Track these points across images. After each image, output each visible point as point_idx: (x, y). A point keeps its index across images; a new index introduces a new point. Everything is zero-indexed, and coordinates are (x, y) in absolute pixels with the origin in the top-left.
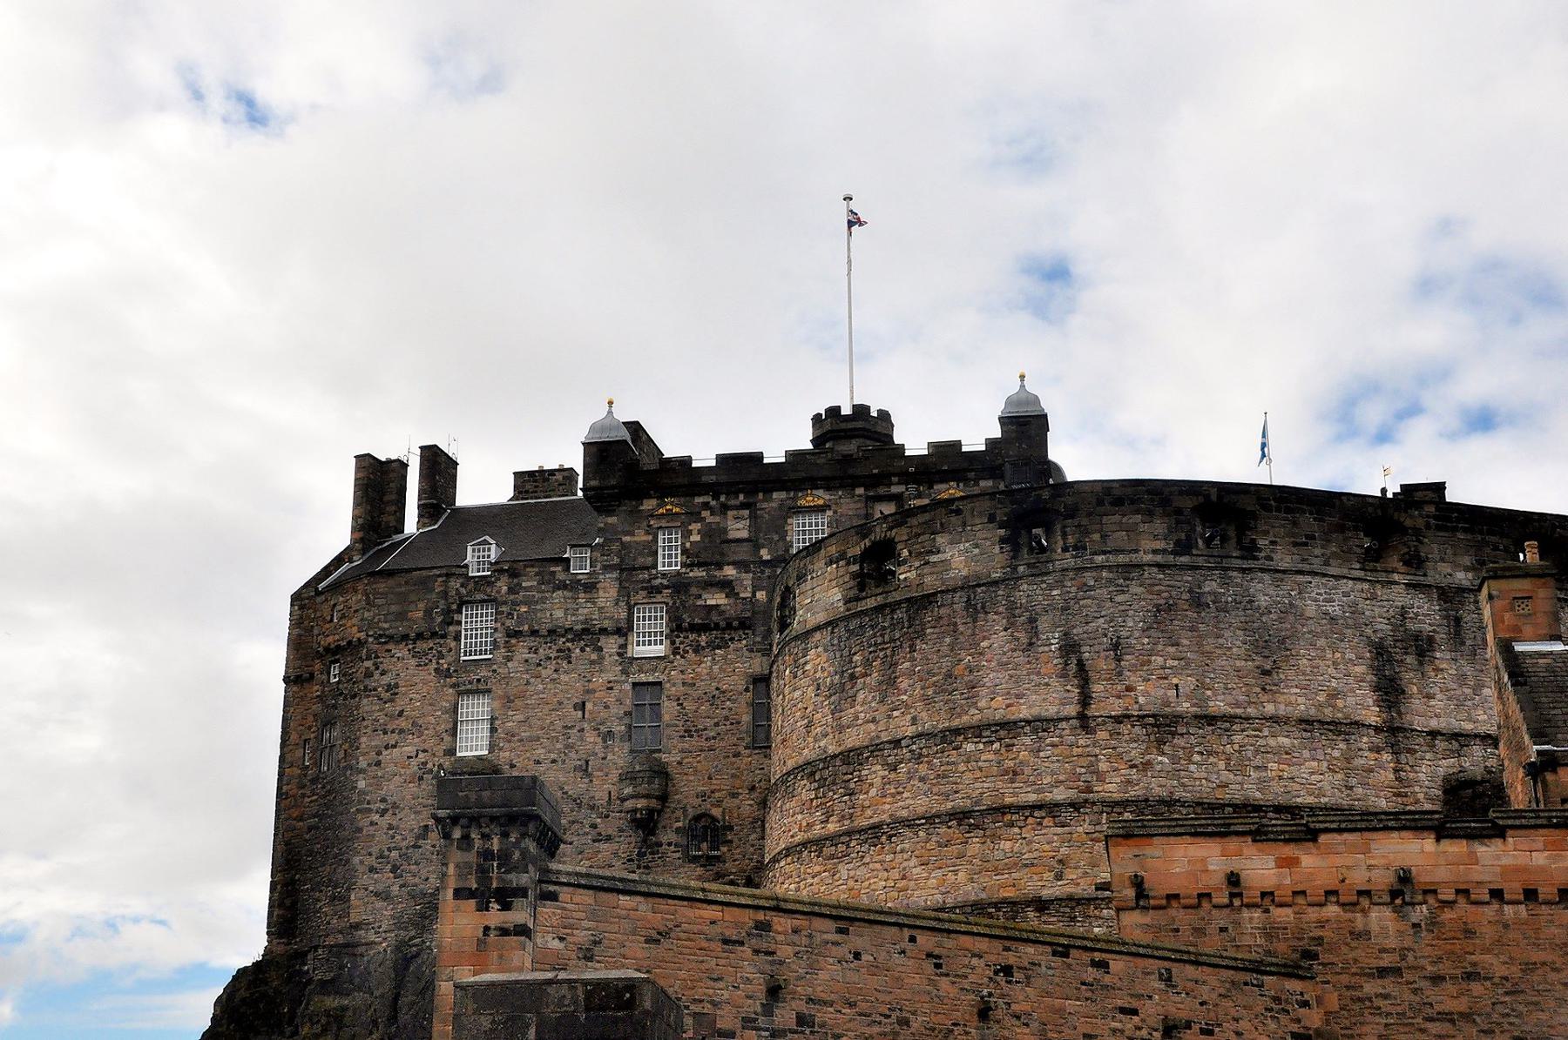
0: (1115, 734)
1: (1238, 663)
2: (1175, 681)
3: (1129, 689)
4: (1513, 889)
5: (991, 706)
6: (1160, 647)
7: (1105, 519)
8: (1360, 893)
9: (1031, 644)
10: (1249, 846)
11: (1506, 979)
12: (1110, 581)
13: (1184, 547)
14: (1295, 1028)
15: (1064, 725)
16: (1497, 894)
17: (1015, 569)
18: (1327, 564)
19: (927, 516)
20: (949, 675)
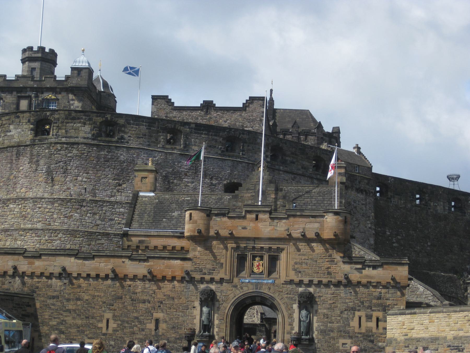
0: (60, 205)
1: (110, 181)
2: (85, 186)
3: (69, 189)
4: (93, 274)
5: (21, 191)
6: (81, 174)
7: (67, 124)
8: (51, 274)
9: (36, 170)
10: (21, 258)
11: (87, 300)
12: (66, 148)
13: (95, 137)
14: (24, 313)
15: (43, 200)
16: (88, 275)
17: (34, 140)
18: (149, 145)
19: (7, 117)
20: (9, 179)
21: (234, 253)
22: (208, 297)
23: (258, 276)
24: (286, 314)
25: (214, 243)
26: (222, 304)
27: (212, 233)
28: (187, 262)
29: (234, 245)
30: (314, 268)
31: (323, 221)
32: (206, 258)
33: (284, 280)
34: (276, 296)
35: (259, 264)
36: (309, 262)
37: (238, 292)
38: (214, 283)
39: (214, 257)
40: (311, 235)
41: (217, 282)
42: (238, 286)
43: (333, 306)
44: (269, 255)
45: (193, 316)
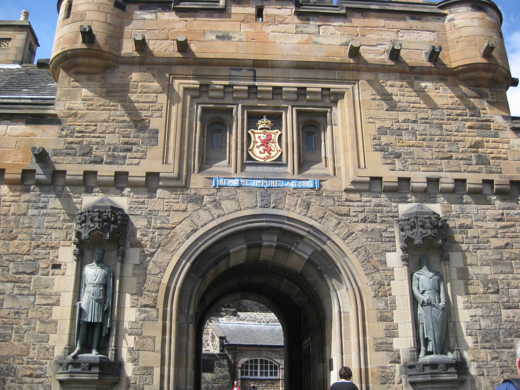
21: (191, 106)
22: (104, 229)
23: (266, 169)
24: (365, 283)
25: (135, 76)
26: (152, 254)
27: (128, 48)
28: (46, 127)
29: (194, 83)
30: (436, 144)
31: (444, 27)
32: (105, 115)
33: (352, 177)
34: (328, 227)
35: (269, 135)
36: (420, 127)
37: (204, 216)
38: (127, 190)
39: (129, 114)
40: (416, 55)
41: (135, 186)
42: (206, 199)
43: (506, 255)
44: (299, 113)
45: (50, 296)
